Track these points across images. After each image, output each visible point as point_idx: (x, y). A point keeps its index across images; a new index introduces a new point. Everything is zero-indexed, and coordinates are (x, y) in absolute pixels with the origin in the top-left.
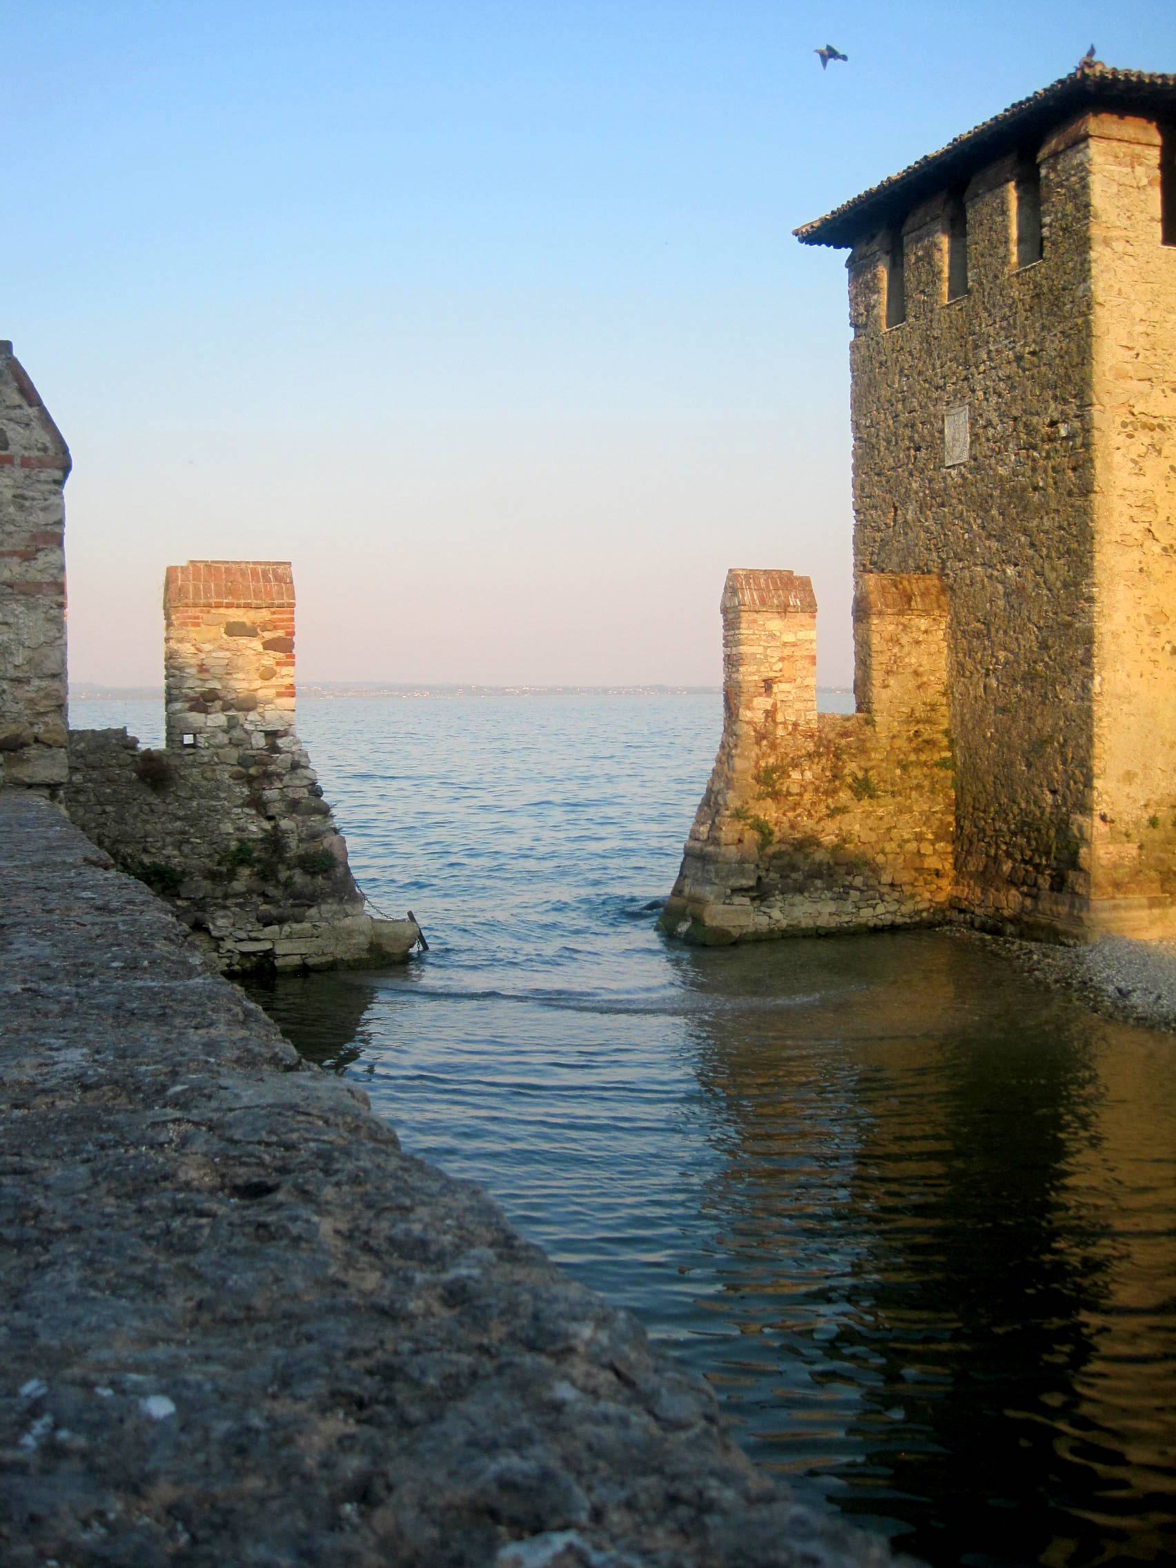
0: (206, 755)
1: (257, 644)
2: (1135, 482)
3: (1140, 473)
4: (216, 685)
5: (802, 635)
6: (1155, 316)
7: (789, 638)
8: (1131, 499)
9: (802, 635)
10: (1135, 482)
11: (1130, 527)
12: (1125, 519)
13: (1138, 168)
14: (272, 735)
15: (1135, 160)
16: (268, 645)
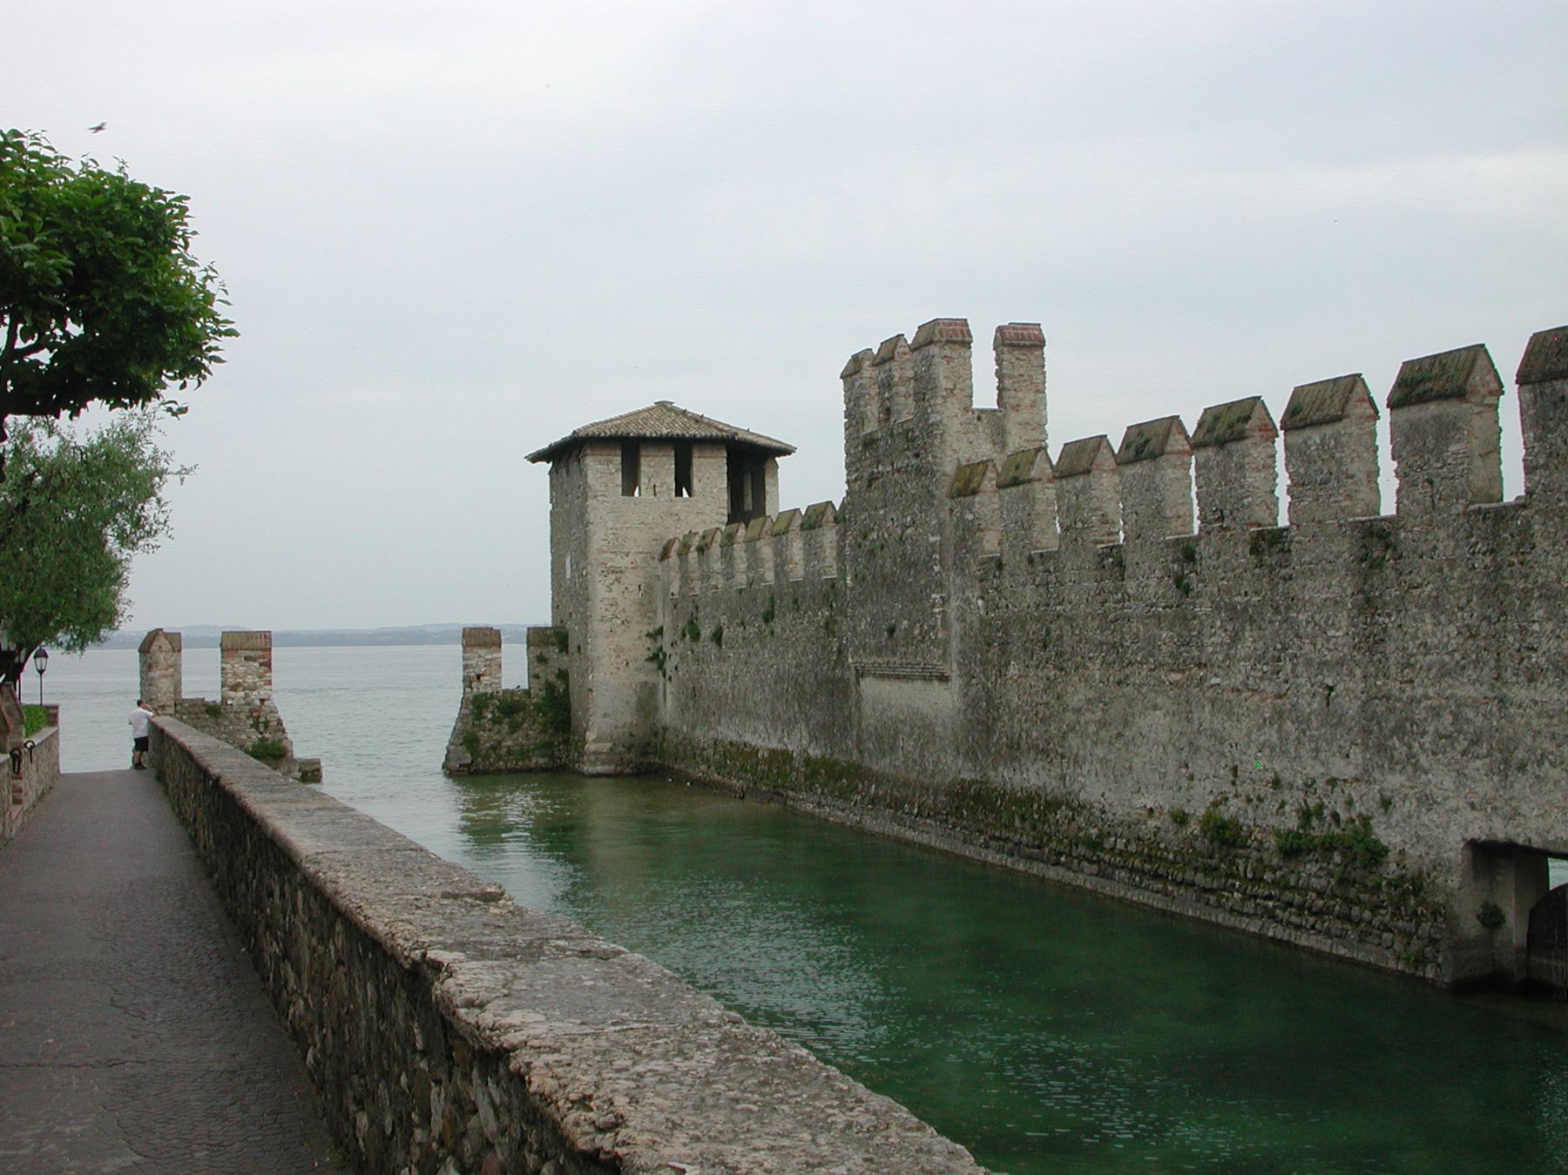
0: (235, 708)
1: (257, 664)
2: (607, 595)
3: (611, 591)
4: (240, 681)
5: (495, 655)
6: (618, 526)
7: (489, 657)
8: (605, 602)
9: (495, 655)
10: (607, 595)
11: (606, 613)
12: (603, 610)
13: (611, 466)
14: (262, 701)
15: (608, 463)
16: (261, 665)
